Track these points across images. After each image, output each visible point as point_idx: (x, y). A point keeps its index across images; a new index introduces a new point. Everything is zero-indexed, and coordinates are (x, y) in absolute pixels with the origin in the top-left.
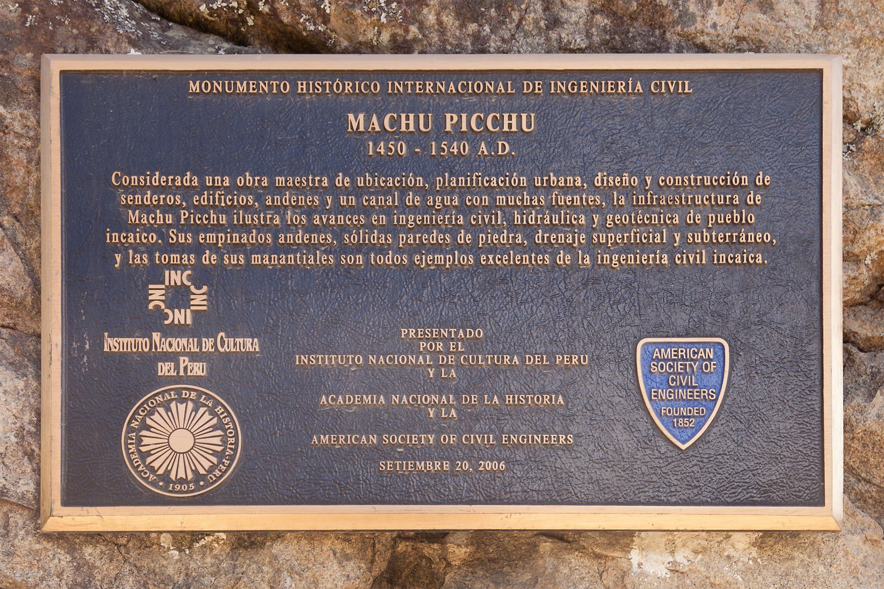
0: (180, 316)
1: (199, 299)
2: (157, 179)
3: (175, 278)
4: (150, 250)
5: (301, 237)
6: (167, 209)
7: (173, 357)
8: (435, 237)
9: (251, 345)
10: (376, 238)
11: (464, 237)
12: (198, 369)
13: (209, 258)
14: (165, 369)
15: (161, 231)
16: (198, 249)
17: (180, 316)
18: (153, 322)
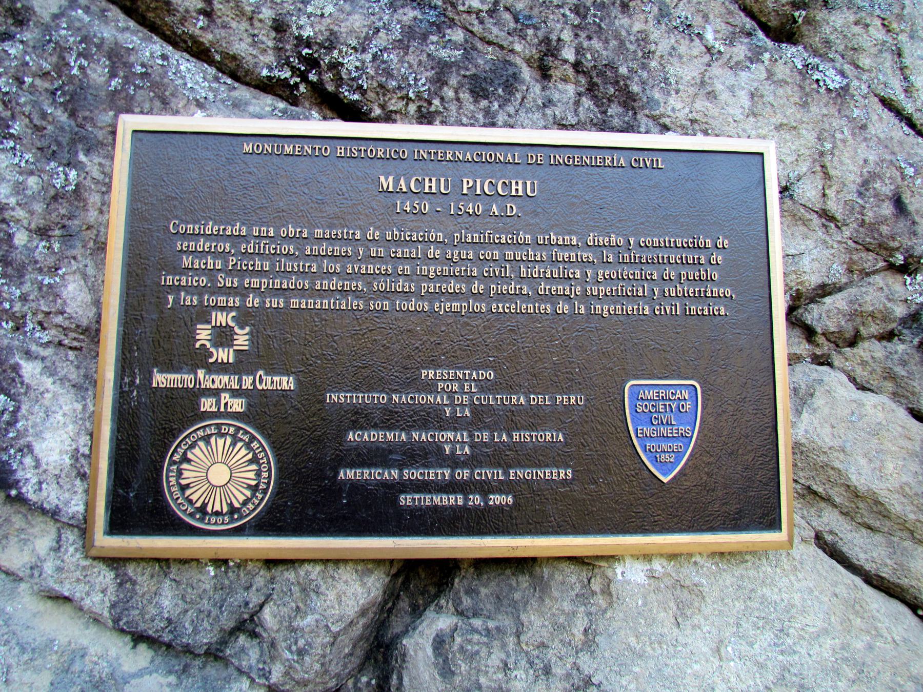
0: (223, 355)
1: (242, 340)
2: (211, 228)
3: (221, 318)
4: (199, 291)
5: (335, 283)
6: (216, 255)
7: (215, 393)
8: (453, 286)
9: (287, 383)
10: (401, 285)
11: (477, 287)
12: (238, 405)
13: (253, 301)
14: (207, 404)
15: (211, 273)
16: (243, 292)
17: (223, 355)
18: (199, 359)
